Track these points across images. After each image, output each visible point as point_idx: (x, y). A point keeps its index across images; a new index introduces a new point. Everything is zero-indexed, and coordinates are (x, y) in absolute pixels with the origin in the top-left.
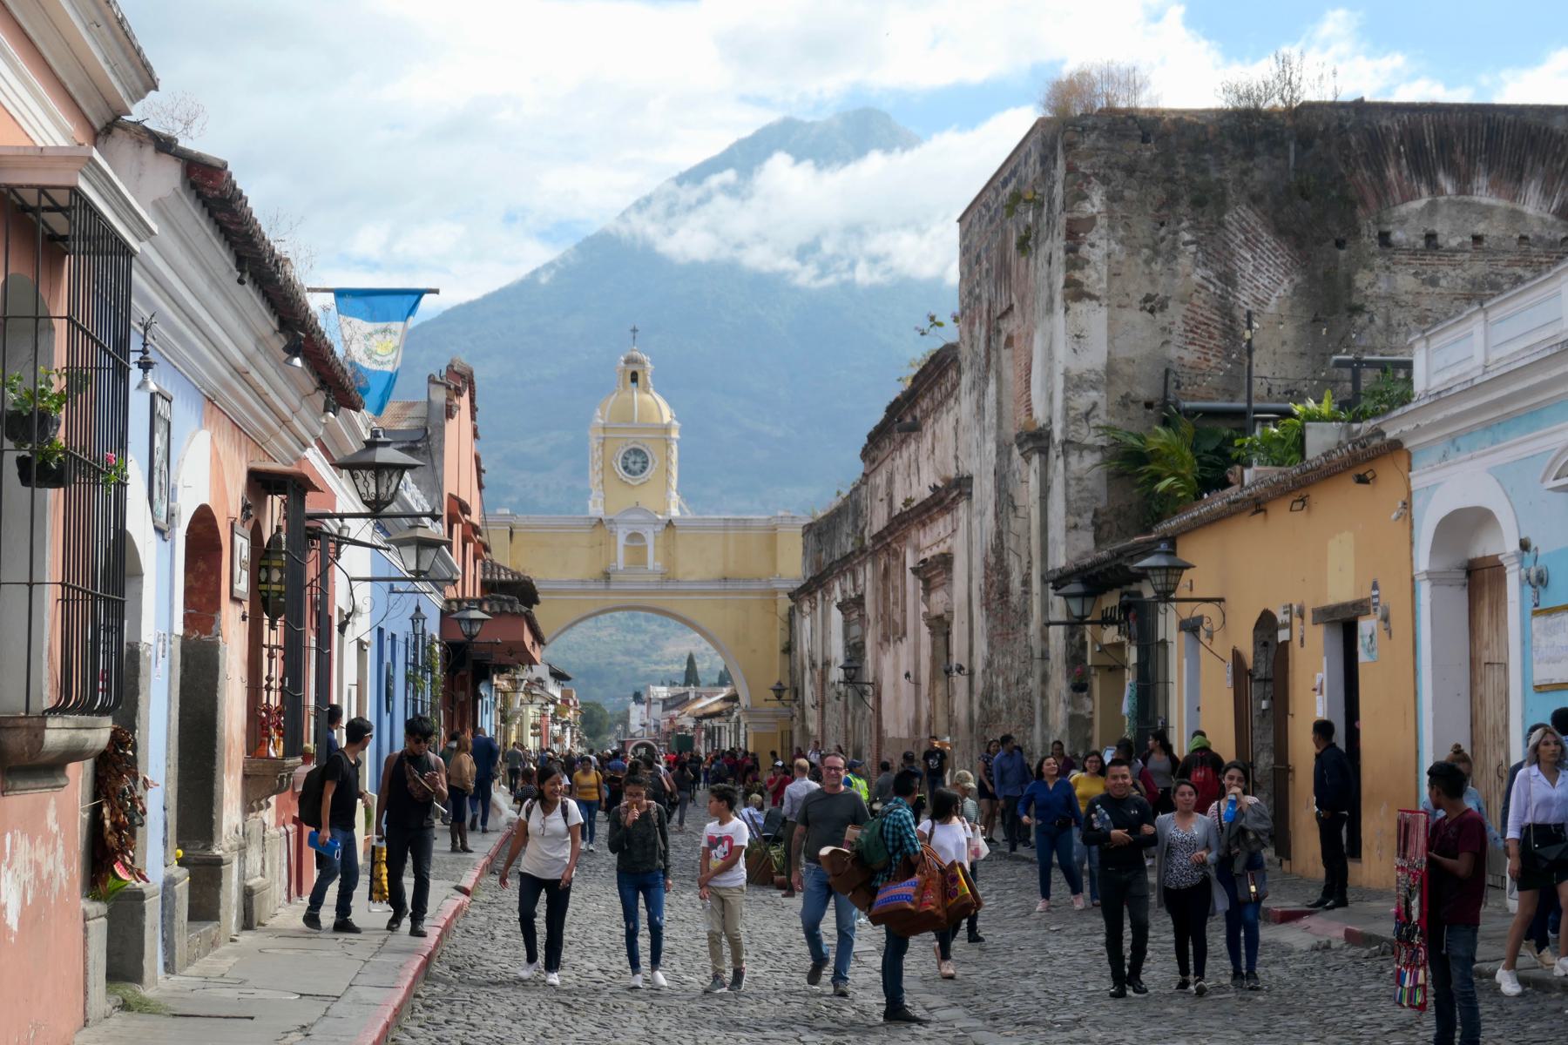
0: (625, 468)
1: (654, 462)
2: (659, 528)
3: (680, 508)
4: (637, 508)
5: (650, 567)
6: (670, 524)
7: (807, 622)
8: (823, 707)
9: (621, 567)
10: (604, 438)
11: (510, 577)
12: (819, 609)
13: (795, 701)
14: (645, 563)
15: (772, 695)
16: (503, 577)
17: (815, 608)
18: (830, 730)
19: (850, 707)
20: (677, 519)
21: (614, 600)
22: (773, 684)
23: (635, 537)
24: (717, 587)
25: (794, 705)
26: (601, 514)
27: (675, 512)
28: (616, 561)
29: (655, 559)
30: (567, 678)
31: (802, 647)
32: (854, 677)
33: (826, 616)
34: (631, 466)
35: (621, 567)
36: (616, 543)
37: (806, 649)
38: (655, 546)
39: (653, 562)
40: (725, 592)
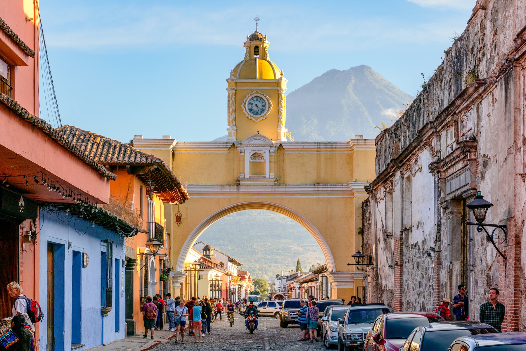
0: (251, 110)
1: (270, 106)
2: (273, 149)
3: (287, 138)
4: (257, 136)
5: (267, 176)
6: (280, 146)
7: (381, 206)
8: (401, 266)
9: (247, 176)
10: (236, 90)
11: (144, 159)
12: (397, 189)
13: (368, 265)
14: (263, 174)
15: (353, 261)
16: (138, 160)
17: (391, 192)
18: (410, 284)
19: (446, 263)
20: (285, 143)
21: (243, 199)
22: (354, 253)
23: (256, 155)
24: (313, 190)
25: (370, 269)
26: (235, 141)
27: (284, 139)
28: (244, 173)
29: (270, 172)
30: (240, 265)
31: (376, 225)
32: (484, 218)
33: (406, 191)
34: (255, 108)
35: (247, 176)
36: (244, 160)
37: (379, 226)
38: (270, 162)
39: (269, 172)
40: (318, 193)
